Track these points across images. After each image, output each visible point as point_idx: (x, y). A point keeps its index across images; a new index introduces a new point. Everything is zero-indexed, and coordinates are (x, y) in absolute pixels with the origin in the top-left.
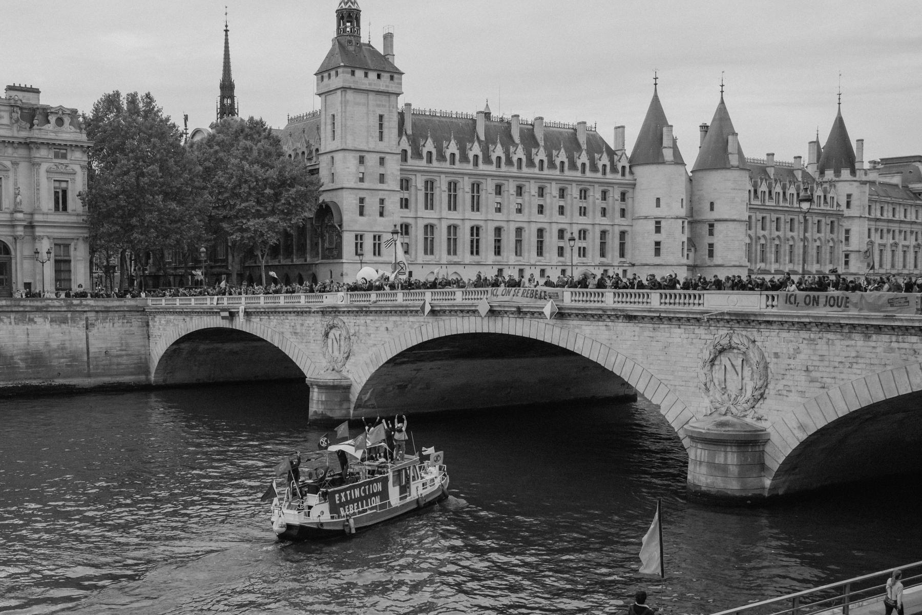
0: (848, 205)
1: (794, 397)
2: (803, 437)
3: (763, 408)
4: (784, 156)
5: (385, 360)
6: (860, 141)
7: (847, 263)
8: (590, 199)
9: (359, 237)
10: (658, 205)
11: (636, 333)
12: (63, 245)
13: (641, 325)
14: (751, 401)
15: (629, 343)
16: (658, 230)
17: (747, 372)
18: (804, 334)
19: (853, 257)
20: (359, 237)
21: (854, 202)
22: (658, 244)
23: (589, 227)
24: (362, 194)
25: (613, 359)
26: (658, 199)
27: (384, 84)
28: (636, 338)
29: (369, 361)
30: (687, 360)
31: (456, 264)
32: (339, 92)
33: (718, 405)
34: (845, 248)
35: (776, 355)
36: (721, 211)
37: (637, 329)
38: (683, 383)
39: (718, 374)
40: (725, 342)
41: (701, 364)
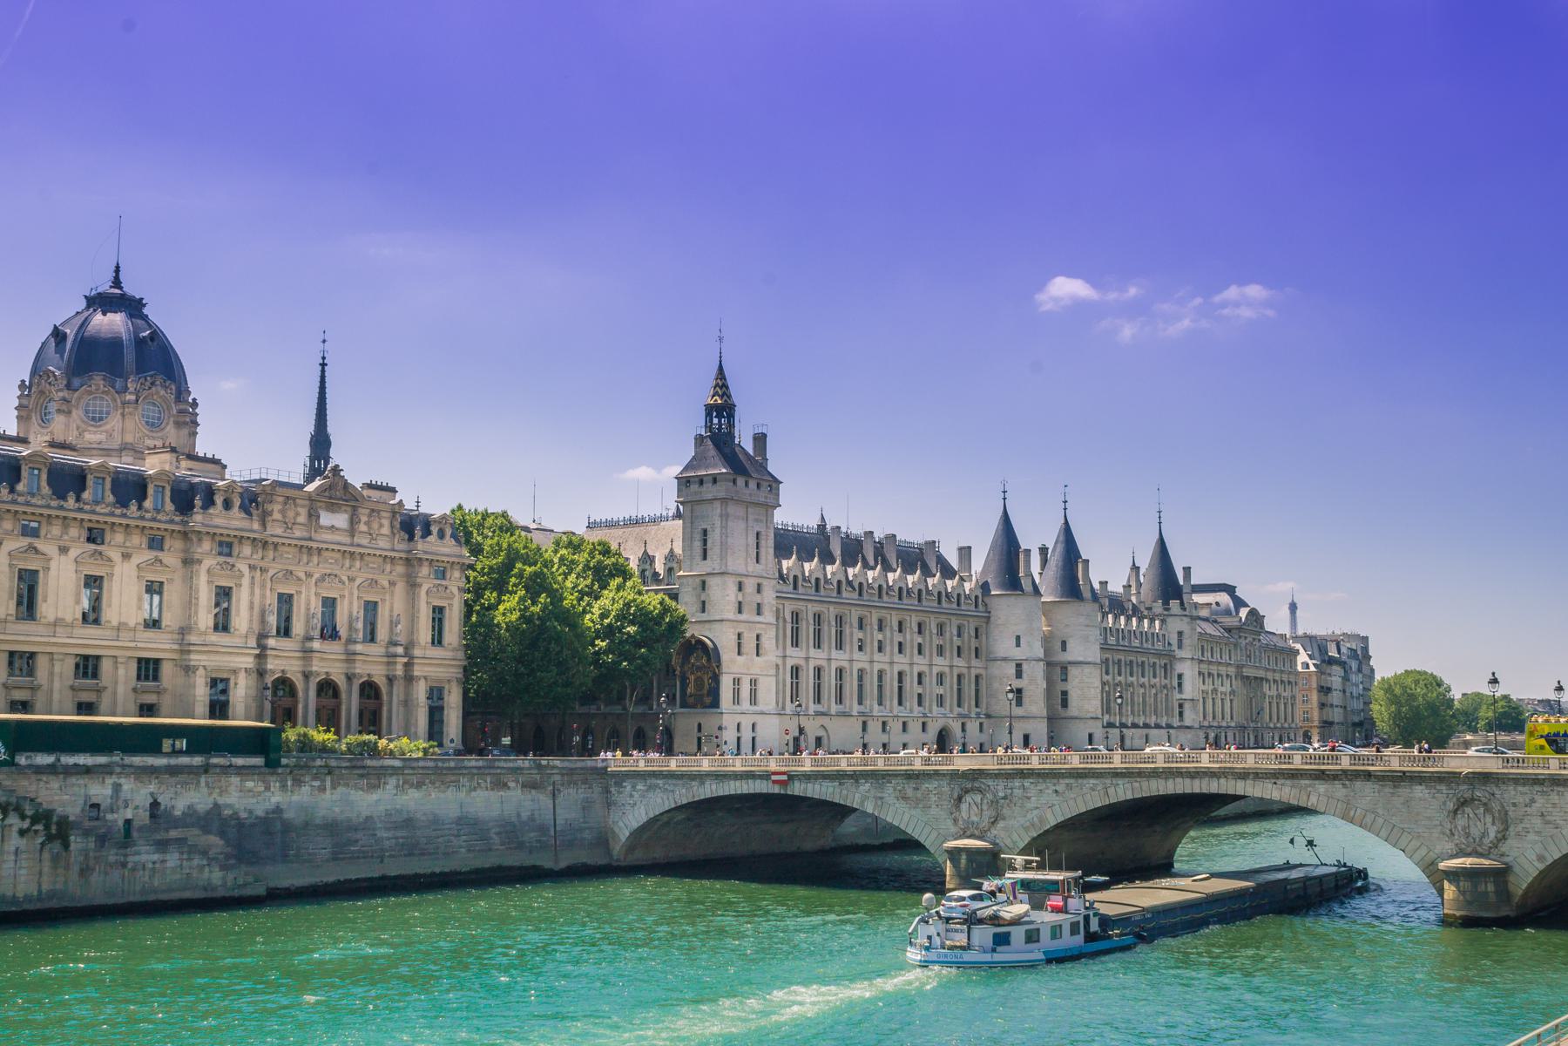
0: (1180, 647)
1: (1531, 837)
2: (1541, 866)
3: (1504, 848)
4: (1116, 587)
5: (1053, 823)
6: (1187, 570)
7: (1181, 714)
8: (948, 635)
9: (737, 681)
10: (1018, 645)
12: (436, 694)
16: (1019, 675)
17: (1489, 819)
18: (1537, 788)
19: (1187, 706)
20: (737, 681)
21: (1186, 642)
22: (1019, 691)
23: (947, 670)
24: (741, 628)
26: (1018, 638)
27: (762, 496)
31: (823, 714)
32: (717, 504)
34: (1179, 696)
35: (1514, 805)
36: (1075, 652)
39: (1461, 822)
40: (1468, 795)
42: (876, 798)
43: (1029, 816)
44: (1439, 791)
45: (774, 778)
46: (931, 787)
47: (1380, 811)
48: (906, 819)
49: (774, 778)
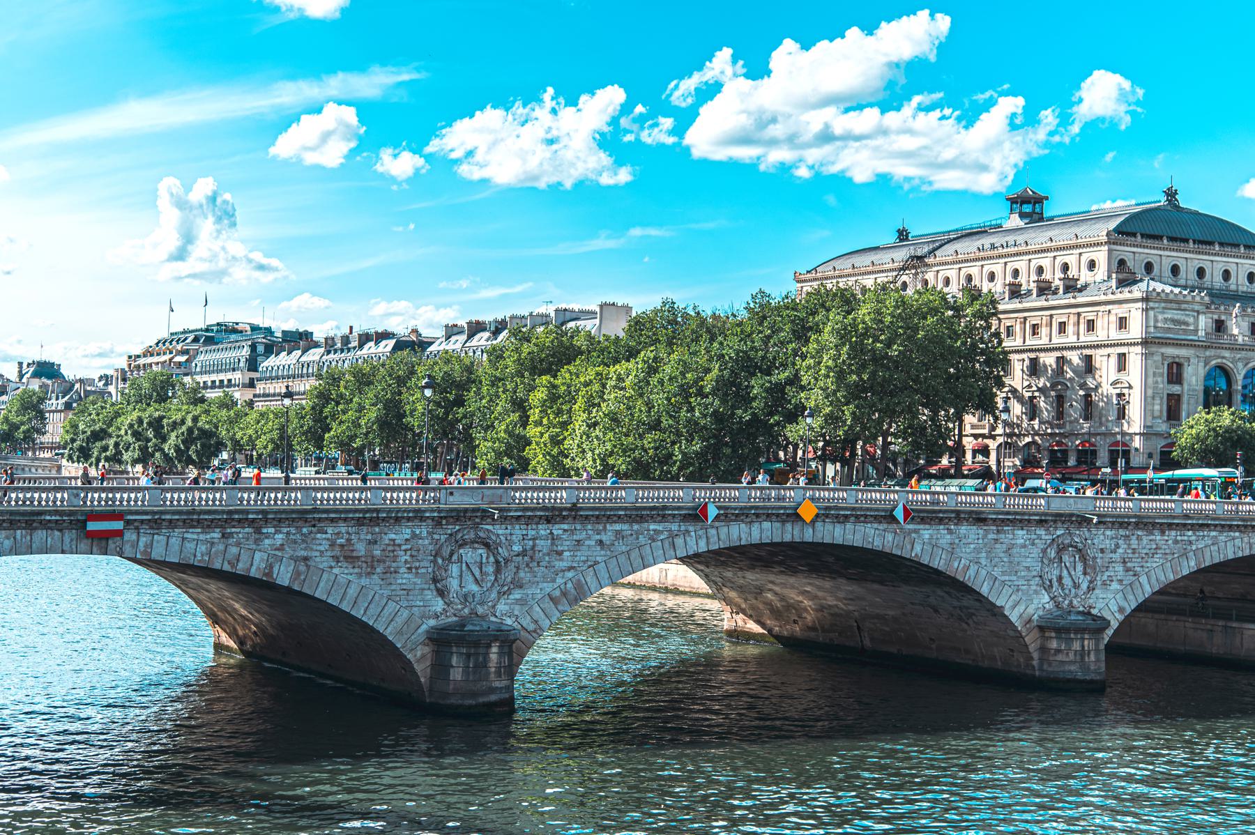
1: (1115, 586)
25: (956, 565)
29: (557, 593)
35: (1102, 551)
42: (296, 559)
43: (559, 581)
45: (92, 526)
46: (399, 539)
47: (983, 562)
48: (352, 592)
49: (92, 526)
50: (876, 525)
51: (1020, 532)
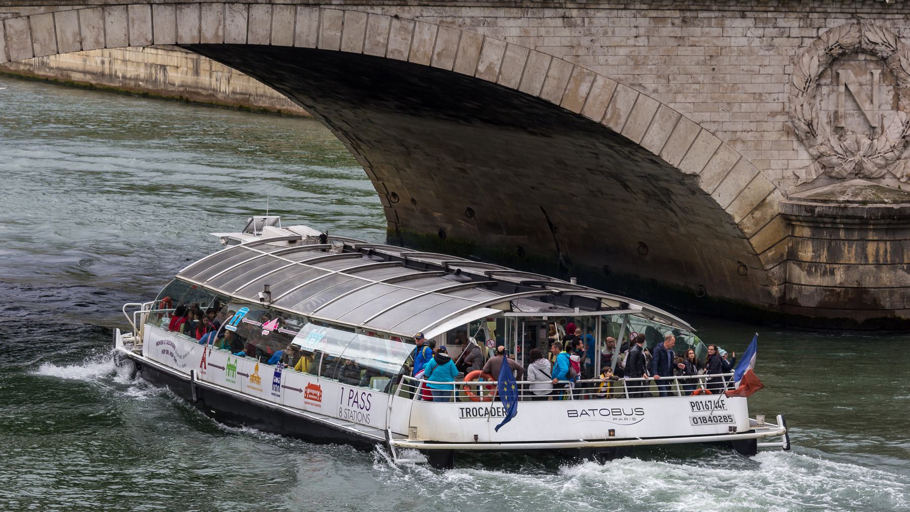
11: (642, 31)
13: (654, 14)
14: (900, 147)
15: (622, 51)
17: (885, 95)
28: (642, 41)
30: (760, 79)
33: (834, 160)
37: (643, 22)
38: (753, 126)
39: (828, 102)
41: (798, 81)
44: (784, 33)
47: (650, 83)
50: (394, 11)
51: (738, 23)
